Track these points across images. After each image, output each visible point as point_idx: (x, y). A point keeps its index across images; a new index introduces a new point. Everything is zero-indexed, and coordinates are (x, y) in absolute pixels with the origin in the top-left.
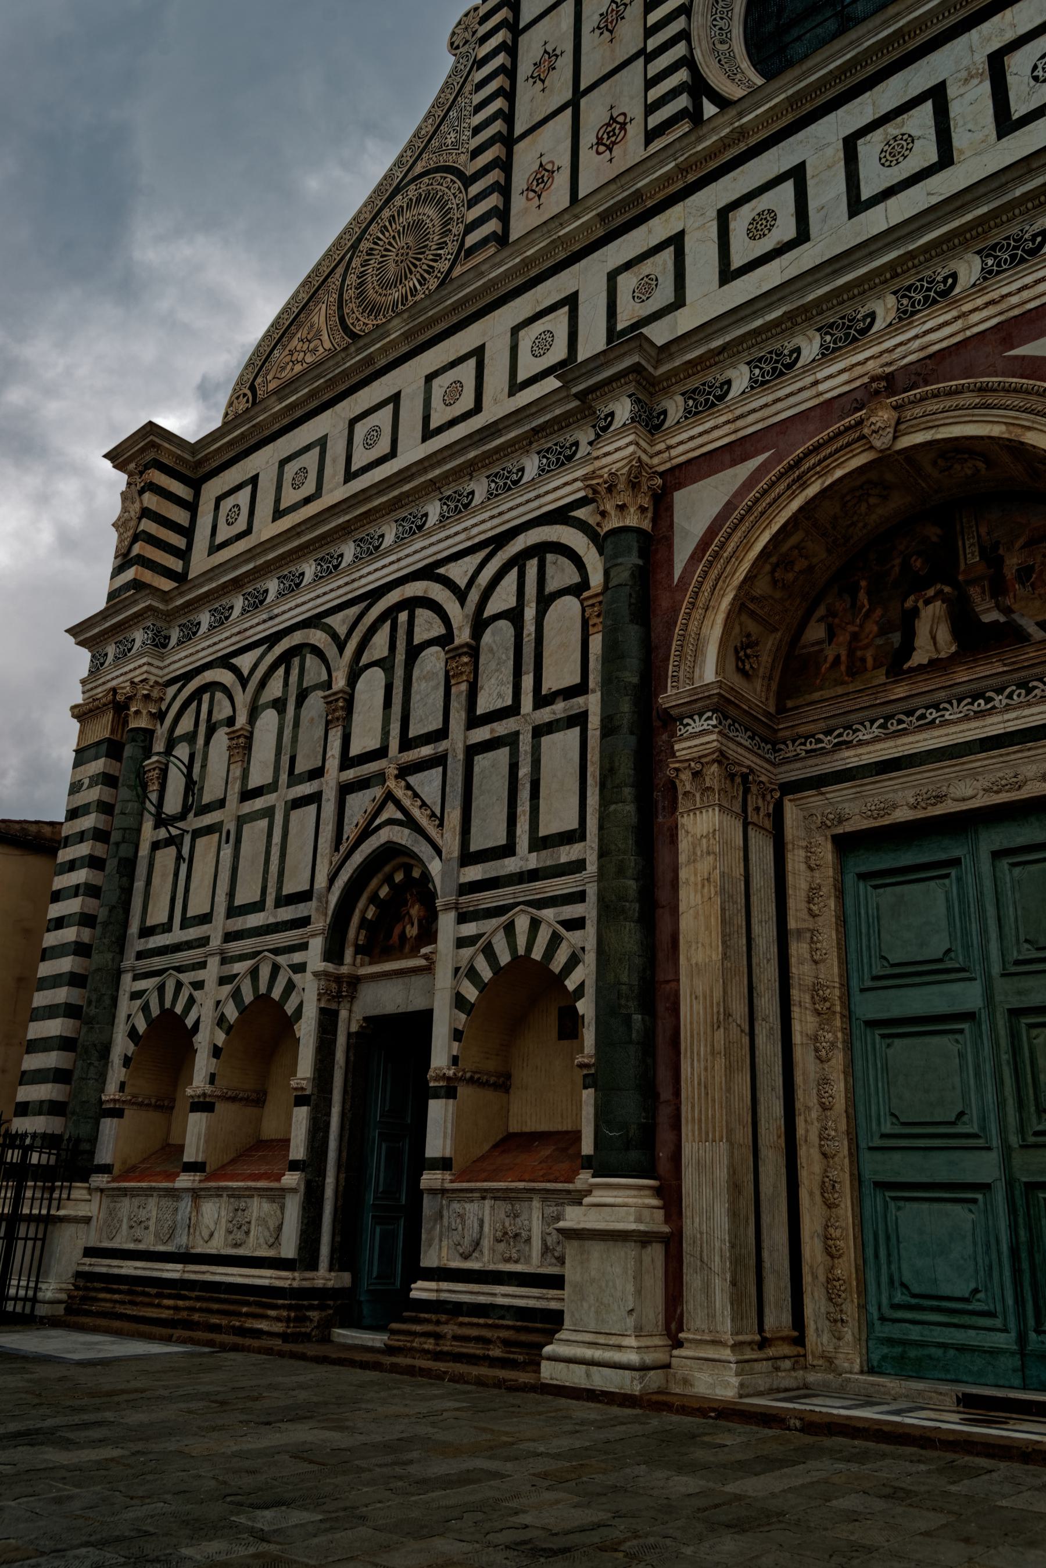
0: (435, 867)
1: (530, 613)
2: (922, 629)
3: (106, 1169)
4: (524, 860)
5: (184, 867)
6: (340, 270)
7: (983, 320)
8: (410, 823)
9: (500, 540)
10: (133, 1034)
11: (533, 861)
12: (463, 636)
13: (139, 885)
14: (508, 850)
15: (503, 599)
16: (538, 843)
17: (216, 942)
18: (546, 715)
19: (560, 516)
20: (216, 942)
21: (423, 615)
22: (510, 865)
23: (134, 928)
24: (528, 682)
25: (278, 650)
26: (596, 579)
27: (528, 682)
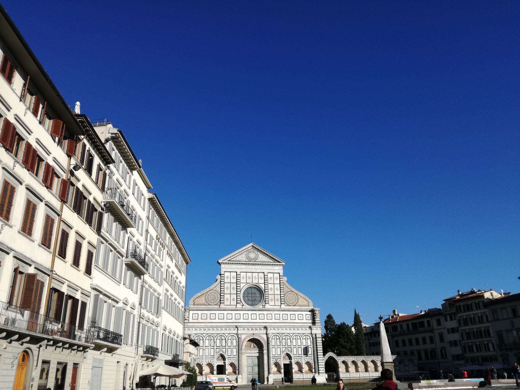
0: (225, 356)
1: (232, 340)
2: (252, 345)
3: (204, 375)
4: (232, 356)
5: (199, 351)
6: (205, 294)
7: (259, 333)
8: (223, 352)
9: (230, 334)
11: (233, 357)
12: (227, 340)
14: (231, 355)
15: (230, 338)
16: (233, 355)
17: (204, 358)
18: (233, 347)
21: (223, 337)
22: (231, 357)
24: (232, 344)
27: (232, 344)
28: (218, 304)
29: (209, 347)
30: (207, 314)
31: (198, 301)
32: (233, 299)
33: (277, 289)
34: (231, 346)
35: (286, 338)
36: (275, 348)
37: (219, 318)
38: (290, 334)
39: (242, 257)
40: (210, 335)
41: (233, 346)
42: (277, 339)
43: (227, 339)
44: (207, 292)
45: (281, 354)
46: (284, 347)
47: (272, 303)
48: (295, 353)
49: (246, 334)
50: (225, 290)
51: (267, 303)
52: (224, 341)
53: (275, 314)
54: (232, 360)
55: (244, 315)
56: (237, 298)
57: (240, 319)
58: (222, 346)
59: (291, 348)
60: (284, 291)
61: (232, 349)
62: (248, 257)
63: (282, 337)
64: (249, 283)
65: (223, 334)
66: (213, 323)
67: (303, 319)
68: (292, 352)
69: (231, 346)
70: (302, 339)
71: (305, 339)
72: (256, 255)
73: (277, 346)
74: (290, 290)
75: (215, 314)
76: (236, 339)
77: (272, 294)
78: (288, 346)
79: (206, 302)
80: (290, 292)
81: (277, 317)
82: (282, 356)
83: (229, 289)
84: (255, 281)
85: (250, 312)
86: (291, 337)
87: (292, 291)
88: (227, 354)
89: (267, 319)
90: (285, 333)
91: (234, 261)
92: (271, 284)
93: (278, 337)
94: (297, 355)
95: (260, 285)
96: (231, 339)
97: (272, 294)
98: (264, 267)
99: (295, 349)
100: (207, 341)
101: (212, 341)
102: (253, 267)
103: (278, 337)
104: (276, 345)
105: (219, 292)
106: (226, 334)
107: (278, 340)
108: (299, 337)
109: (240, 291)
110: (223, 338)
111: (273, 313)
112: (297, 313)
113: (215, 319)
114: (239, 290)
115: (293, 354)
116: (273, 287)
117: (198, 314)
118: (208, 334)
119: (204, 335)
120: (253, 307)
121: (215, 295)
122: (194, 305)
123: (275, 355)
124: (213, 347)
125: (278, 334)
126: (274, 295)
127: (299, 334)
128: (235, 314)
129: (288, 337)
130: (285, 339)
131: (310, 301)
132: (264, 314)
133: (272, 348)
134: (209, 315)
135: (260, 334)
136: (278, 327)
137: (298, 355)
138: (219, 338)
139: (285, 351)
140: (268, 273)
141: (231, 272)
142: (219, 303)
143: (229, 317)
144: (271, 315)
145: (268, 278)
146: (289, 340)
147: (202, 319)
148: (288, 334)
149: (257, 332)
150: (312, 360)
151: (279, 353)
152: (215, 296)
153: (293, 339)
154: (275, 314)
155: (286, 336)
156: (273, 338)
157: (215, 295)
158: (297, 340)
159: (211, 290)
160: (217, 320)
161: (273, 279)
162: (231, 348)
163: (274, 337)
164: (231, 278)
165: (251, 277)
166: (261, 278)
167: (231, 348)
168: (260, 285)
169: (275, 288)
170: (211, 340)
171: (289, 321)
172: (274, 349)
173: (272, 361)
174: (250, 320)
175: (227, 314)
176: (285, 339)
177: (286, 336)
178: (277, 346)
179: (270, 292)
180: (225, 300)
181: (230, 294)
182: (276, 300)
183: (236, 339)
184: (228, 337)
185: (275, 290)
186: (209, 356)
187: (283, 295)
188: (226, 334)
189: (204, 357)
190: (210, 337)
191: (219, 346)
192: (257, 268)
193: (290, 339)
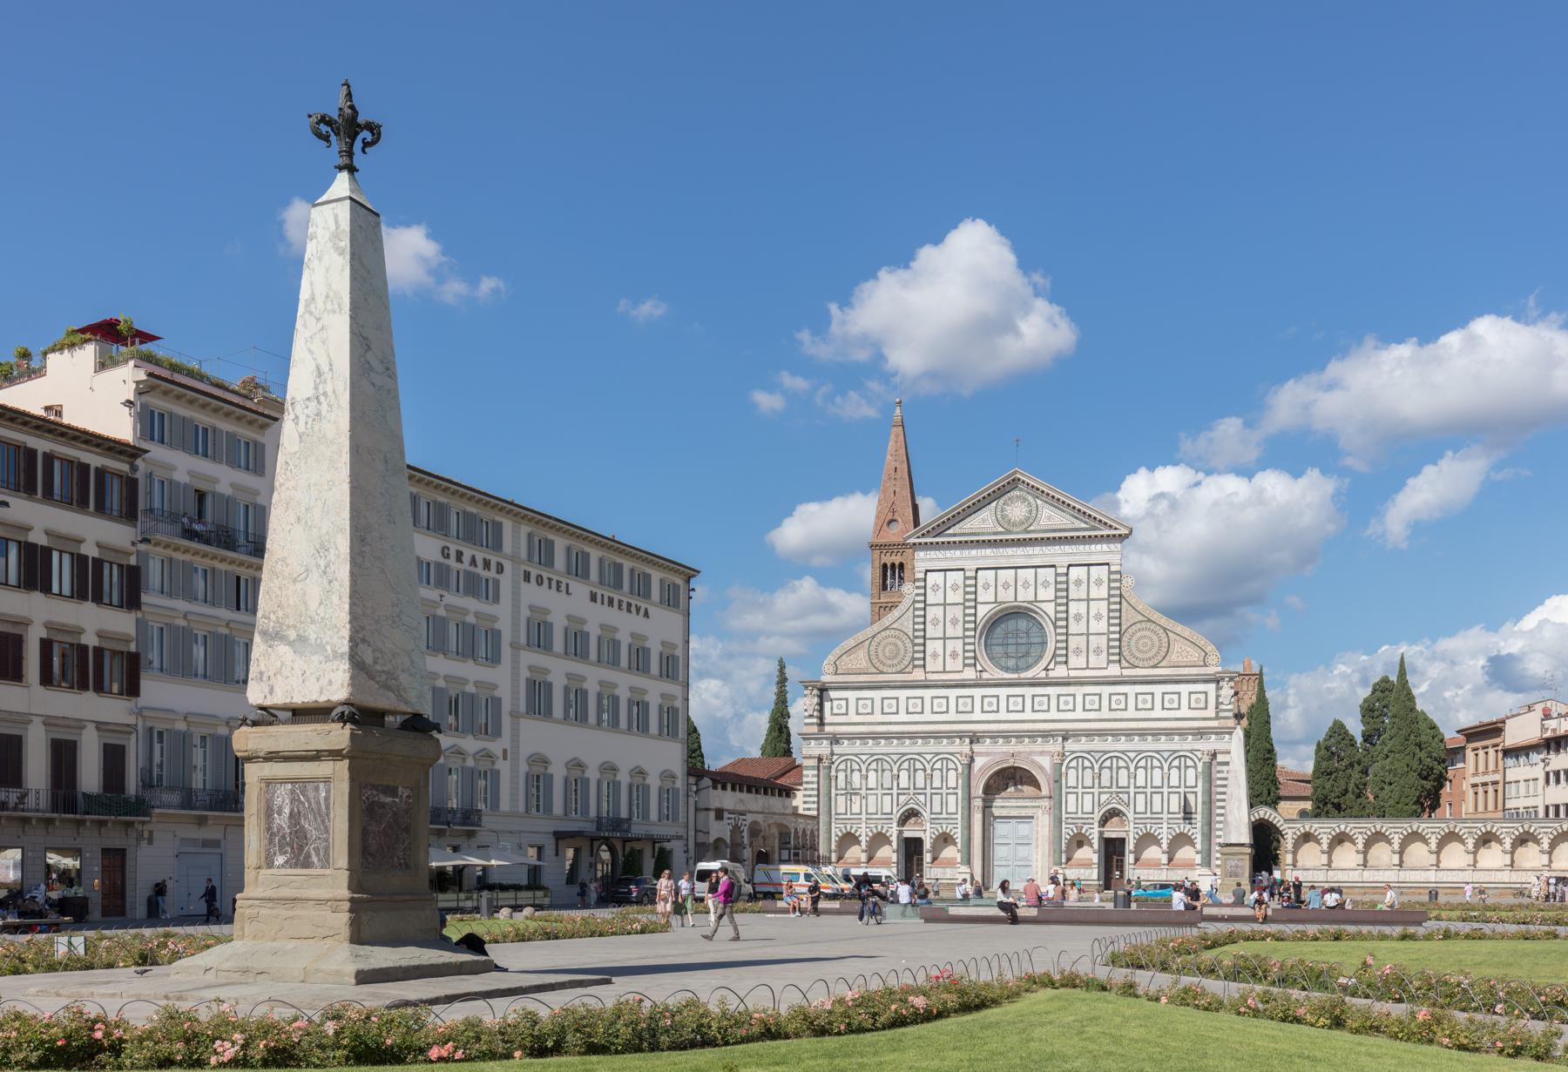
0: (924, 813)
1: (944, 771)
4: (944, 816)
6: (868, 642)
7: (1028, 750)
9: (937, 754)
10: (837, 835)
12: (929, 772)
13: (833, 803)
14: (941, 813)
15: (938, 765)
16: (947, 813)
19: (952, 754)
20: (864, 819)
23: (833, 813)
25: (875, 757)
26: (960, 770)
28: (907, 670)
29: (877, 789)
30: (872, 699)
31: (847, 663)
32: (954, 655)
33: (1098, 617)
34: (941, 788)
35: (1114, 766)
36: (1077, 793)
37: (907, 709)
38: (1128, 754)
39: (984, 521)
40: (880, 757)
41: (948, 788)
42: (1084, 768)
43: (928, 767)
44: (873, 637)
45: (1096, 810)
46: (1105, 790)
47: (1074, 661)
48: (1140, 808)
49: (987, 754)
50: (929, 627)
51: (1060, 663)
52: (920, 774)
53: (1085, 695)
54: (944, 826)
55: (986, 700)
56: (965, 651)
57: (972, 712)
58: (915, 789)
59: (1128, 793)
60: (1123, 622)
61: (944, 795)
62: (1002, 519)
63: (1100, 762)
64: (1005, 603)
65: (919, 754)
66: (890, 723)
67: (1179, 709)
68: (1132, 806)
69: (941, 788)
70: (1166, 766)
71: (1179, 768)
72: (1031, 510)
73: (1083, 787)
74: (1141, 618)
75: (897, 699)
76: (956, 770)
77: (1082, 634)
78: (1118, 787)
79: (870, 665)
80: (1144, 625)
81: (1092, 703)
82: (1097, 816)
83: (941, 624)
84: (1025, 596)
85: (1003, 692)
86: (1132, 761)
87: (1149, 620)
88: (928, 810)
89: (1058, 710)
90: (1110, 752)
91: (955, 535)
92: (1079, 600)
93: (1087, 764)
94: (1146, 813)
95: (1042, 605)
96: (941, 770)
97: (1082, 634)
98: (1057, 549)
99: (1140, 798)
100: (872, 775)
101: (887, 774)
102: (1020, 551)
103: (1087, 764)
104: (1080, 786)
105: (910, 634)
106: (925, 756)
107: (1088, 772)
108: (1156, 763)
109: (975, 630)
110: (918, 765)
111: (1080, 691)
112: (1158, 689)
113: (897, 713)
114: (972, 626)
115: (1132, 812)
116: (1083, 611)
117: (847, 699)
118: (873, 755)
119: (864, 758)
120: (1016, 676)
121: (900, 643)
122: (836, 674)
123: (1077, 813)
124: (889, 789)
125: (1088, 752)
126: (1088, 635)
127: (1157, 752)
128: (957, 697)
129: (1121, 763)
130: (1111, 768)
131: (1210, 648)
132: (1048, 696)
133: (1067, 793)
134: (878, 703)
135: (1031, 753)
136: (1090, 734)
137: (1149, 815)
138: (906, 765)
139: (1109, 804)
140: (1070, 566)
141: (945, 570)
142: (911, 666)
143: (940, 705)
144: (1072, 698)
145: (1070, 582)
146: (1123, 772)
147: (858, 714)
148: (1123, 752)
149: (1022, 750)
150: (1195, 830)
151: (1088, 808)
152: (896, 645)
153: (1136, 768)
154: (1085, 695)
155: (1115, 760)
156: (1071, 765)
157: (900, 643)
158: (1149, 771)
159: (884, 630)
160: (903, 717)
161: (1084, 586)
162: (941, 794)
163: (1074, 764)
164: (948, 590)
165: (1013, 583)
166: (1046, 584)
167: (941, 794)
168: (1042, 605)
169: (1092, 614)
170: (883, 771)
171: (1131, 713)
172: (1072, 798)
173: (1064, 830)
174: (1003, 715)
175: (933, 698)
176: (1111, 768)
177: (1115, 760)
178: (1083, 787)
179: (1073, 629)
180: (928, 658)
181: (945, 638)
182: (1091, 649)
183: (956, 770)
184: (931, 763)
185: (1091, 620)
186: (879, 812)
187: (1117, 636)
188: (925, 756)
189: (864, 816)
190: (880, 762)
191: (907, 786)
192: (1031, 552)
193: (1127, 768)
